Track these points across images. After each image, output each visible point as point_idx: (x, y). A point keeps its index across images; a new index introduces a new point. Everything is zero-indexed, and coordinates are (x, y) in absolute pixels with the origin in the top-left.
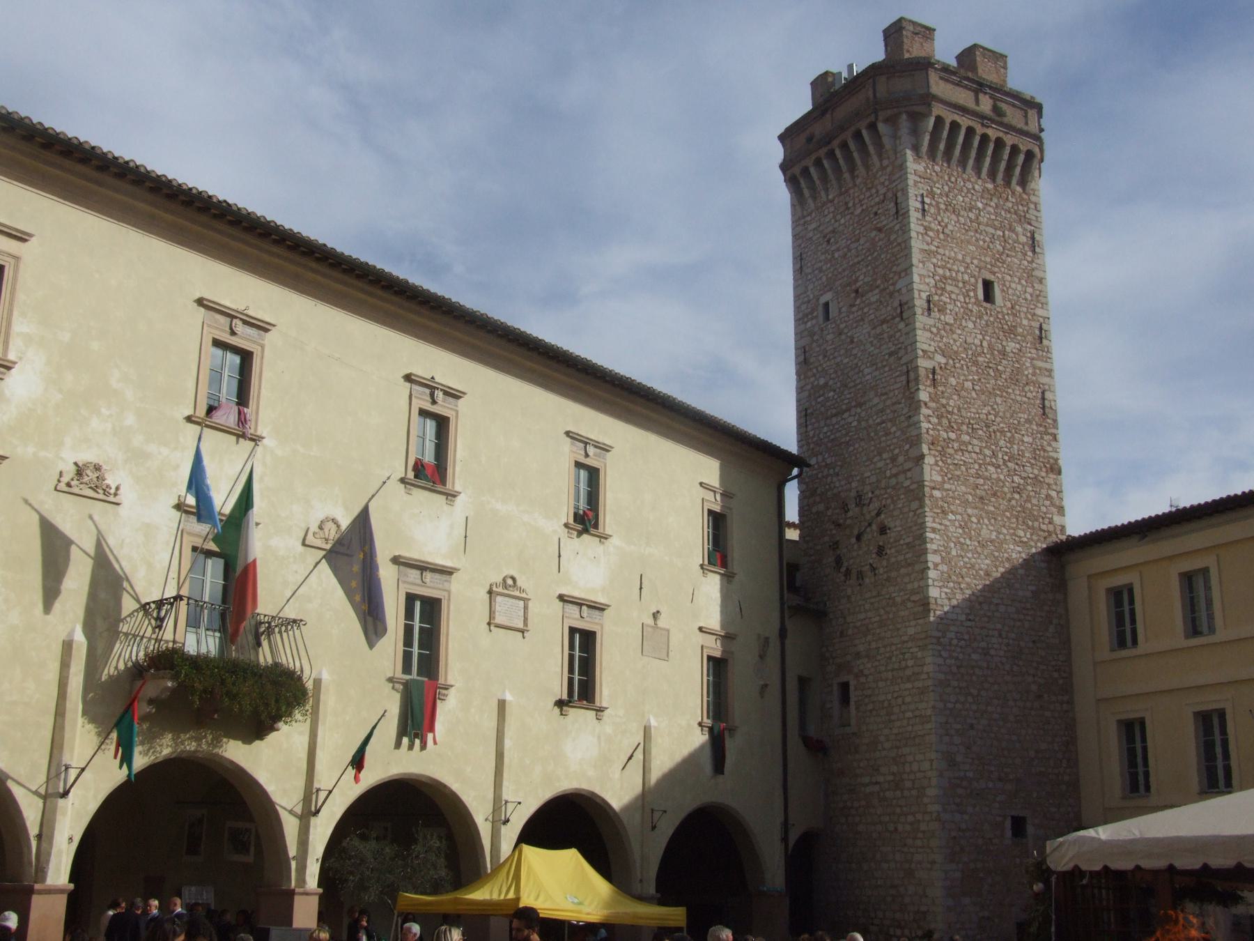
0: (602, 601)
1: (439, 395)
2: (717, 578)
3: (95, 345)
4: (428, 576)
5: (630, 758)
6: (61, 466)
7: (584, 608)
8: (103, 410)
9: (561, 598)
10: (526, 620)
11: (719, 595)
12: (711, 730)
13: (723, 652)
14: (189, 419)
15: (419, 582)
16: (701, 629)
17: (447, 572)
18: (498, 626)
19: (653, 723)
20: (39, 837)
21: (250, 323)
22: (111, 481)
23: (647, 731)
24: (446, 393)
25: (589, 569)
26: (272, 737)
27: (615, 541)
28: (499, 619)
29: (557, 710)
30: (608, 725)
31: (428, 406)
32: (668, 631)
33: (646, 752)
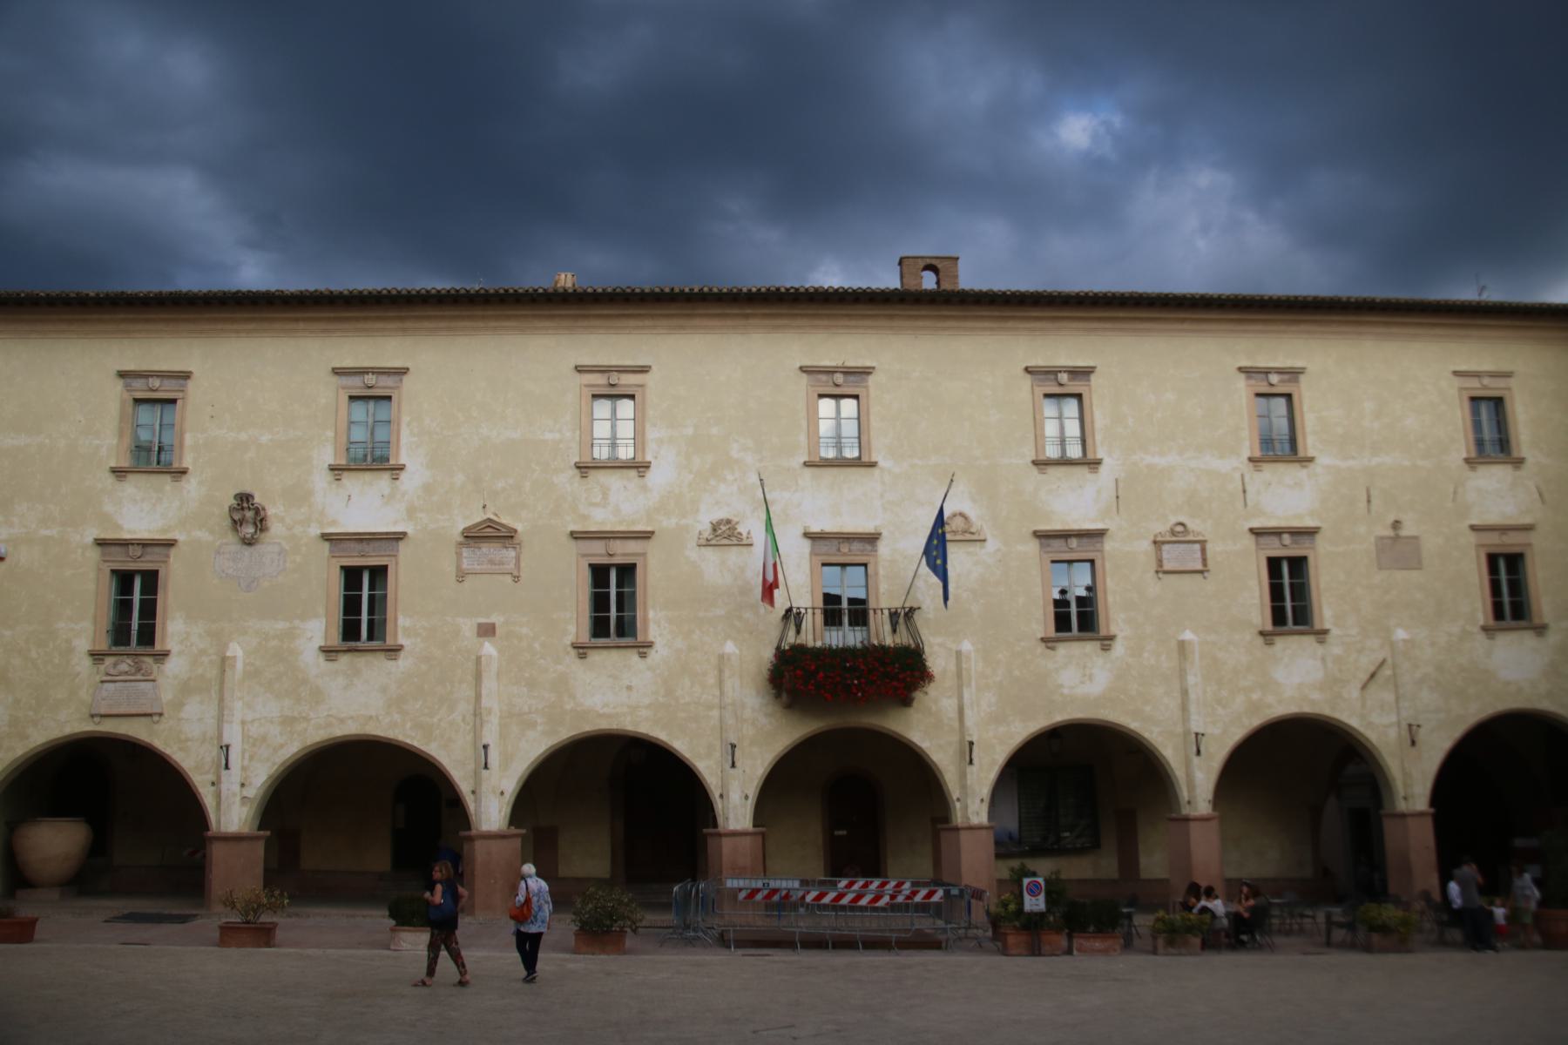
3: (714, 431)
4: (1074, 542)
5: (1373, 676)
6: (700, 527)
8: (730, 477)
10: (1204, 561)
14: (806, 464)
17: (1099, 534)
20: (721, 796)
21: (849, 372)
22: (741, 529)
25: (1287, 498)
26: (915, 704)
27: (1323, 460)
28: (1167, 567)
29: (1260, 640)
30: (1335, 648)
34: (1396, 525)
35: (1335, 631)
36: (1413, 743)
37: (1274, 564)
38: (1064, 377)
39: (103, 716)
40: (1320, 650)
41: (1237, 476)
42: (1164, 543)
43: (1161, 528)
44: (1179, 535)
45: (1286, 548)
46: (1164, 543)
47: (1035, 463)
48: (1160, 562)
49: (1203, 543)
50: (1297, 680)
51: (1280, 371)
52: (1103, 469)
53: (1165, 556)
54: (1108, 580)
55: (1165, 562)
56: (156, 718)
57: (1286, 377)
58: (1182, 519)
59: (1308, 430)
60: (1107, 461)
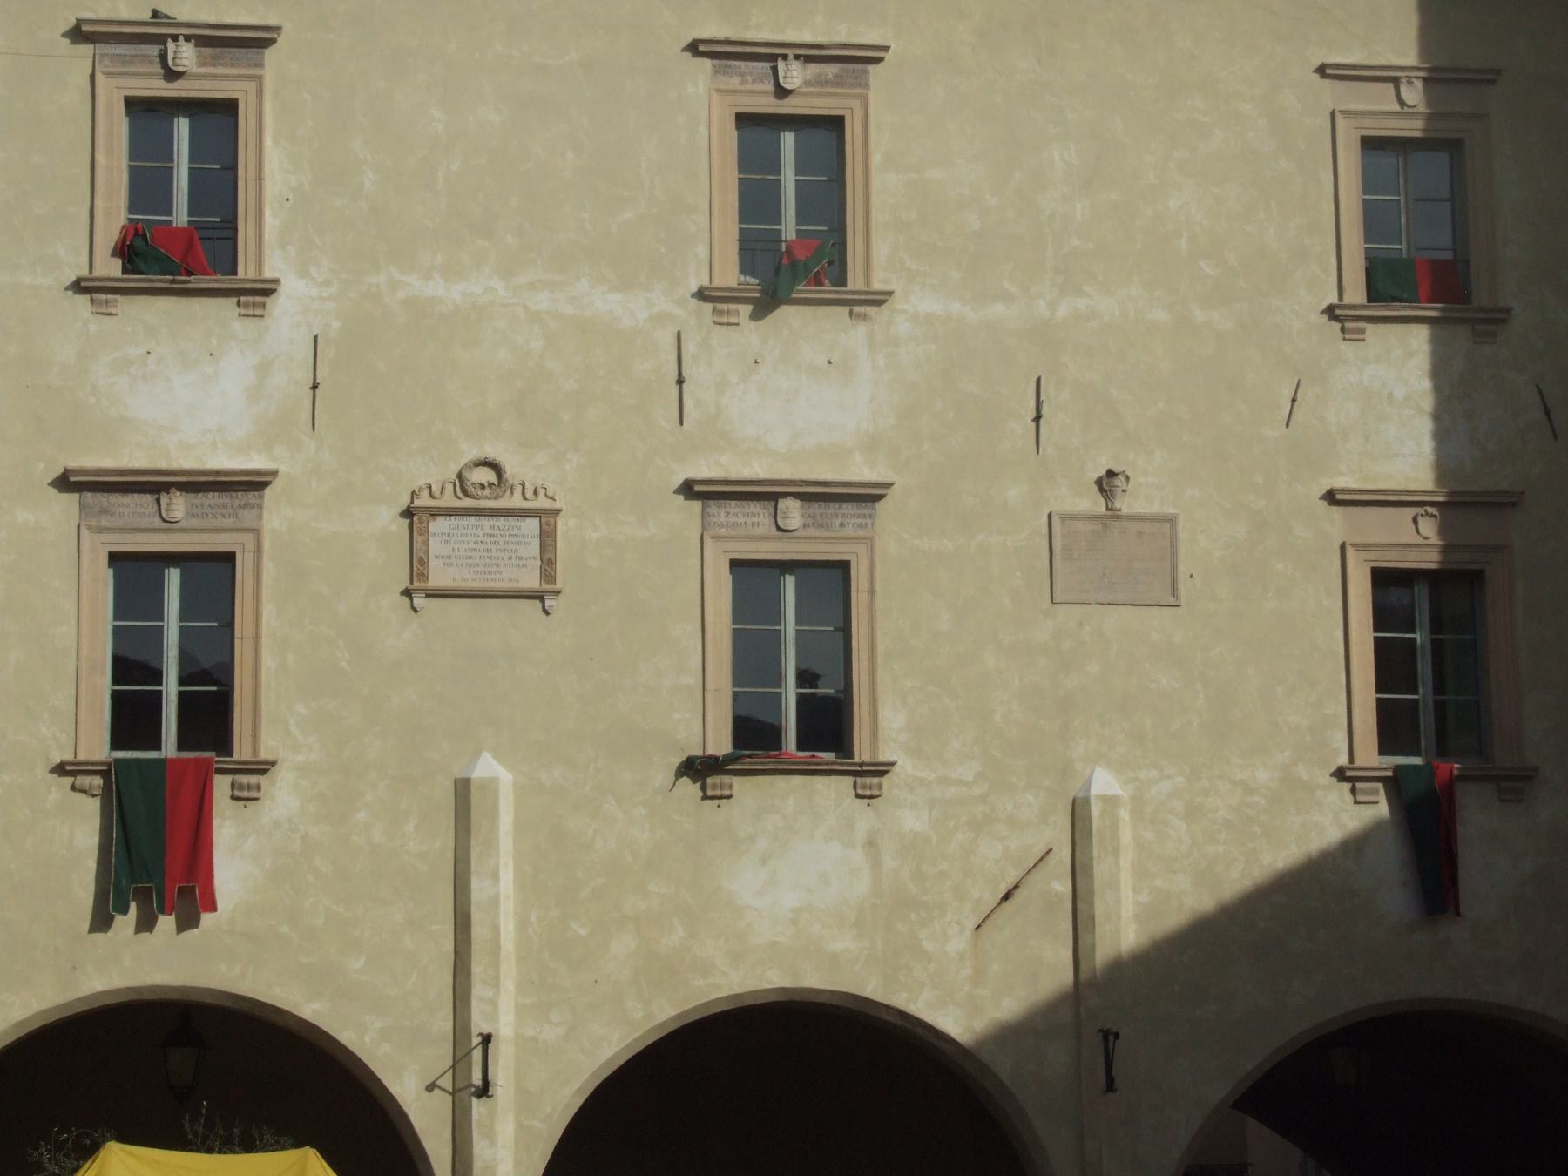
0: (868, 475)
1: (185, 55)
2: (1418, 339)
4: (179, 505)
7: (791, 507)
9: (688, 489)
11: (1427, 384)
12: (1395, 784)
13: (1446, 550)
15: (157, 522)
16: (1331, 497)
17: (254, 484)
18: (434, 594)
19: (1103, 782)
23: (1079, 814)
24: (202, 41)
25: (798, 397)
27: (919, 303)
28: (439, 577)
29: (689, 788)
30: (906, 811)
31: (158, 88)
32: (1171, 520)
33: (1079, 871)
34: (1107, 483)
35: (905, 767)
36: (1110, 1086)
37: (753, 579)
38: (185, 55)
40: (864, 818)
41: (667, 341)
42: (435, 513)
43: (430, 472)
44: (482, 492)
45: (804, 536)
46: (435, 513)
47: (79, 287)
48: (417, 564)
49: (547, 517)
50: (805, 901)
51: (812, 55)
52: (279, 305)
53: (435, 547)
54: (268, 610)
55: (434, 564)
57: (831, 70)
58: (490, 453)
59: (878, 217)
60: (294, 291)
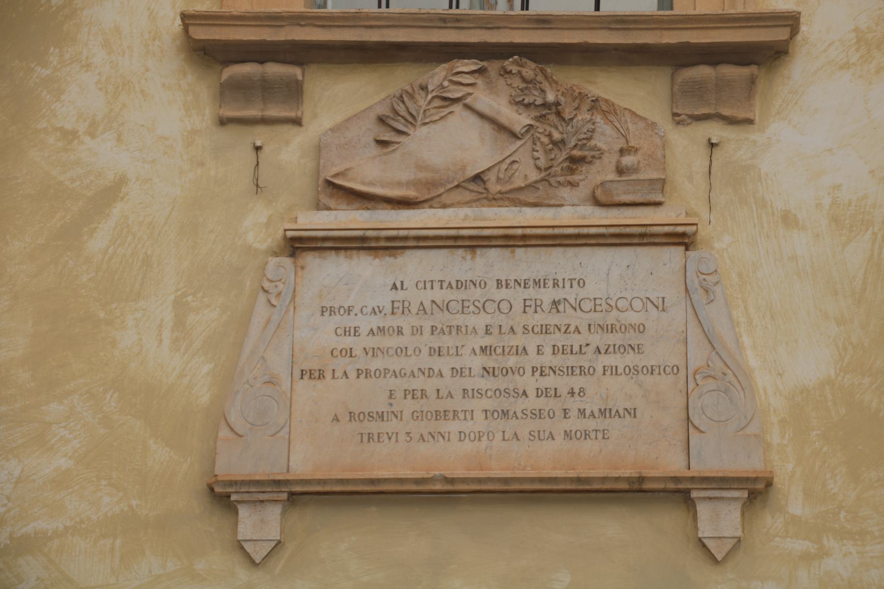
39: (301, 496)
56: (719, 520)
